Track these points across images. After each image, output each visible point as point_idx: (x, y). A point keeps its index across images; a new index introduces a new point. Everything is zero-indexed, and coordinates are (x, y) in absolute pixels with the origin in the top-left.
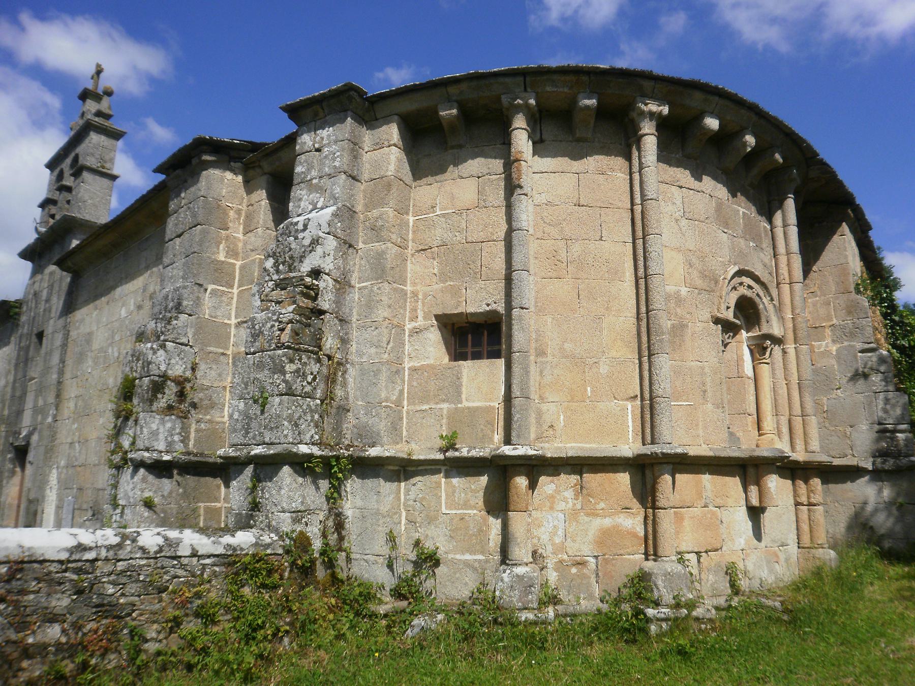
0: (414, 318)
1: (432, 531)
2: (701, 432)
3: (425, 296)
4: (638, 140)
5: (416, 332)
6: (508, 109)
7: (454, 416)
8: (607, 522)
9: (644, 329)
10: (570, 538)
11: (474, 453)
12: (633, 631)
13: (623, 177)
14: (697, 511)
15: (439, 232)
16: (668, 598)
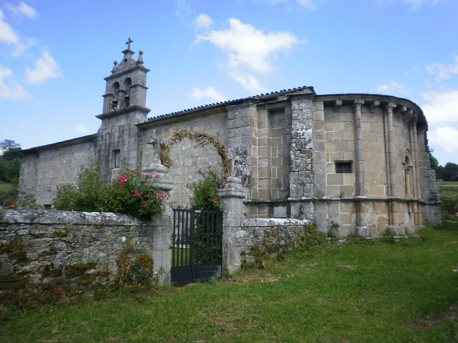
0: (328, 161)
1: (336, 219)
2: (400, 193)
3: (331, 155)
4: (388, 114)
5: (329, 165)
6: (356, 104)
7: (342, 188)
8: (380, 216)
9: (388, 166)
10: (373, 219)
11: (349, 198)
12: (392, 241)
13: (381, 124)
14: (399, 213)
15: (334, 137)
16: (398, 234)
